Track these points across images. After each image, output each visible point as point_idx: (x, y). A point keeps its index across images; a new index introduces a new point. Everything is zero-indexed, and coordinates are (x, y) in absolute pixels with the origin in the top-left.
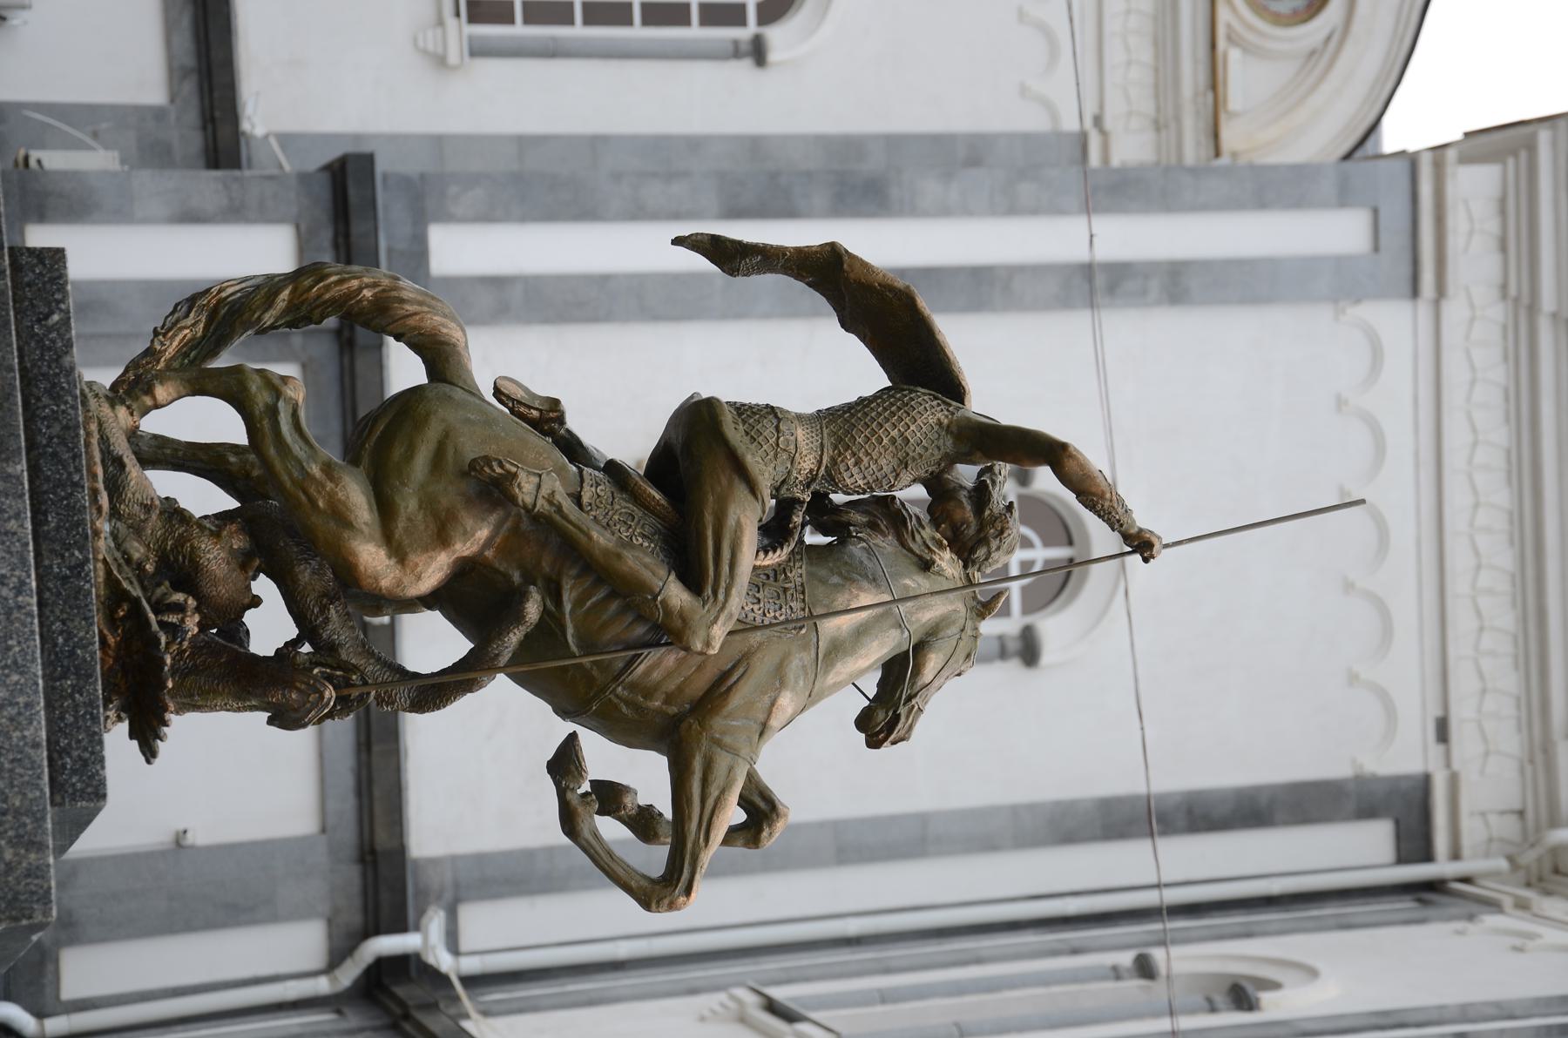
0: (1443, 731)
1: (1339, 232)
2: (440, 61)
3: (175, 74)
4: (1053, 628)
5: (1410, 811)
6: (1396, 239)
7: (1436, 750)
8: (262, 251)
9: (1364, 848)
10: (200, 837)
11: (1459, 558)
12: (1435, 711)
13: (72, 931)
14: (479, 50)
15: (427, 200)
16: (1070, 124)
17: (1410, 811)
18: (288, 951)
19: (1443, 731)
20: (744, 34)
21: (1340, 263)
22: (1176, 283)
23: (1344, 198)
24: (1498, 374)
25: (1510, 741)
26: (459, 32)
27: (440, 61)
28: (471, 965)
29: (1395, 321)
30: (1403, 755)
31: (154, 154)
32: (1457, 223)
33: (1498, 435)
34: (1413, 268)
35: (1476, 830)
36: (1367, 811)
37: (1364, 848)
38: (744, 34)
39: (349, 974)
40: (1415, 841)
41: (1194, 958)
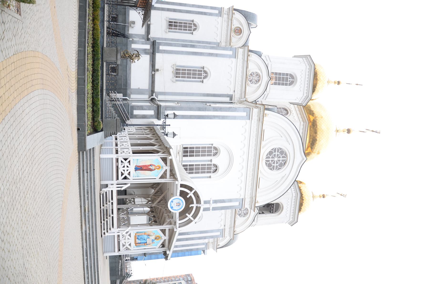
0: (234, 91)
1: (230, 53)
3: (145, 32)
4: (204, 80)
5: (231, 97)
6: (234, 54)
8: (148, 47)
10: (140, 88)
11: (237, 78)
13: (131, 93)
14: (169, 32)
15: (160, 44)
16: (218, 42)
17: (231, 97)
18: (146, 97)
19: (234, 91)
20: (191, 32)
21: (230, 55)
22: (217, 55)
23: (230, 50)
24: (242, 65)
25: (239, 93)
26: (168, 30)
28: (158, 99)
29: (234, 60)
30: (231, 93)
31: (143, 38)
32: (239, 53)
33: (241, 69)
34: (235, 56)
35: (235, 99)
36: (228, 97)
37: (227, 99)
38: (191, 32)
39: (150, 99)
40: (231, 99)
41: (208, 104)
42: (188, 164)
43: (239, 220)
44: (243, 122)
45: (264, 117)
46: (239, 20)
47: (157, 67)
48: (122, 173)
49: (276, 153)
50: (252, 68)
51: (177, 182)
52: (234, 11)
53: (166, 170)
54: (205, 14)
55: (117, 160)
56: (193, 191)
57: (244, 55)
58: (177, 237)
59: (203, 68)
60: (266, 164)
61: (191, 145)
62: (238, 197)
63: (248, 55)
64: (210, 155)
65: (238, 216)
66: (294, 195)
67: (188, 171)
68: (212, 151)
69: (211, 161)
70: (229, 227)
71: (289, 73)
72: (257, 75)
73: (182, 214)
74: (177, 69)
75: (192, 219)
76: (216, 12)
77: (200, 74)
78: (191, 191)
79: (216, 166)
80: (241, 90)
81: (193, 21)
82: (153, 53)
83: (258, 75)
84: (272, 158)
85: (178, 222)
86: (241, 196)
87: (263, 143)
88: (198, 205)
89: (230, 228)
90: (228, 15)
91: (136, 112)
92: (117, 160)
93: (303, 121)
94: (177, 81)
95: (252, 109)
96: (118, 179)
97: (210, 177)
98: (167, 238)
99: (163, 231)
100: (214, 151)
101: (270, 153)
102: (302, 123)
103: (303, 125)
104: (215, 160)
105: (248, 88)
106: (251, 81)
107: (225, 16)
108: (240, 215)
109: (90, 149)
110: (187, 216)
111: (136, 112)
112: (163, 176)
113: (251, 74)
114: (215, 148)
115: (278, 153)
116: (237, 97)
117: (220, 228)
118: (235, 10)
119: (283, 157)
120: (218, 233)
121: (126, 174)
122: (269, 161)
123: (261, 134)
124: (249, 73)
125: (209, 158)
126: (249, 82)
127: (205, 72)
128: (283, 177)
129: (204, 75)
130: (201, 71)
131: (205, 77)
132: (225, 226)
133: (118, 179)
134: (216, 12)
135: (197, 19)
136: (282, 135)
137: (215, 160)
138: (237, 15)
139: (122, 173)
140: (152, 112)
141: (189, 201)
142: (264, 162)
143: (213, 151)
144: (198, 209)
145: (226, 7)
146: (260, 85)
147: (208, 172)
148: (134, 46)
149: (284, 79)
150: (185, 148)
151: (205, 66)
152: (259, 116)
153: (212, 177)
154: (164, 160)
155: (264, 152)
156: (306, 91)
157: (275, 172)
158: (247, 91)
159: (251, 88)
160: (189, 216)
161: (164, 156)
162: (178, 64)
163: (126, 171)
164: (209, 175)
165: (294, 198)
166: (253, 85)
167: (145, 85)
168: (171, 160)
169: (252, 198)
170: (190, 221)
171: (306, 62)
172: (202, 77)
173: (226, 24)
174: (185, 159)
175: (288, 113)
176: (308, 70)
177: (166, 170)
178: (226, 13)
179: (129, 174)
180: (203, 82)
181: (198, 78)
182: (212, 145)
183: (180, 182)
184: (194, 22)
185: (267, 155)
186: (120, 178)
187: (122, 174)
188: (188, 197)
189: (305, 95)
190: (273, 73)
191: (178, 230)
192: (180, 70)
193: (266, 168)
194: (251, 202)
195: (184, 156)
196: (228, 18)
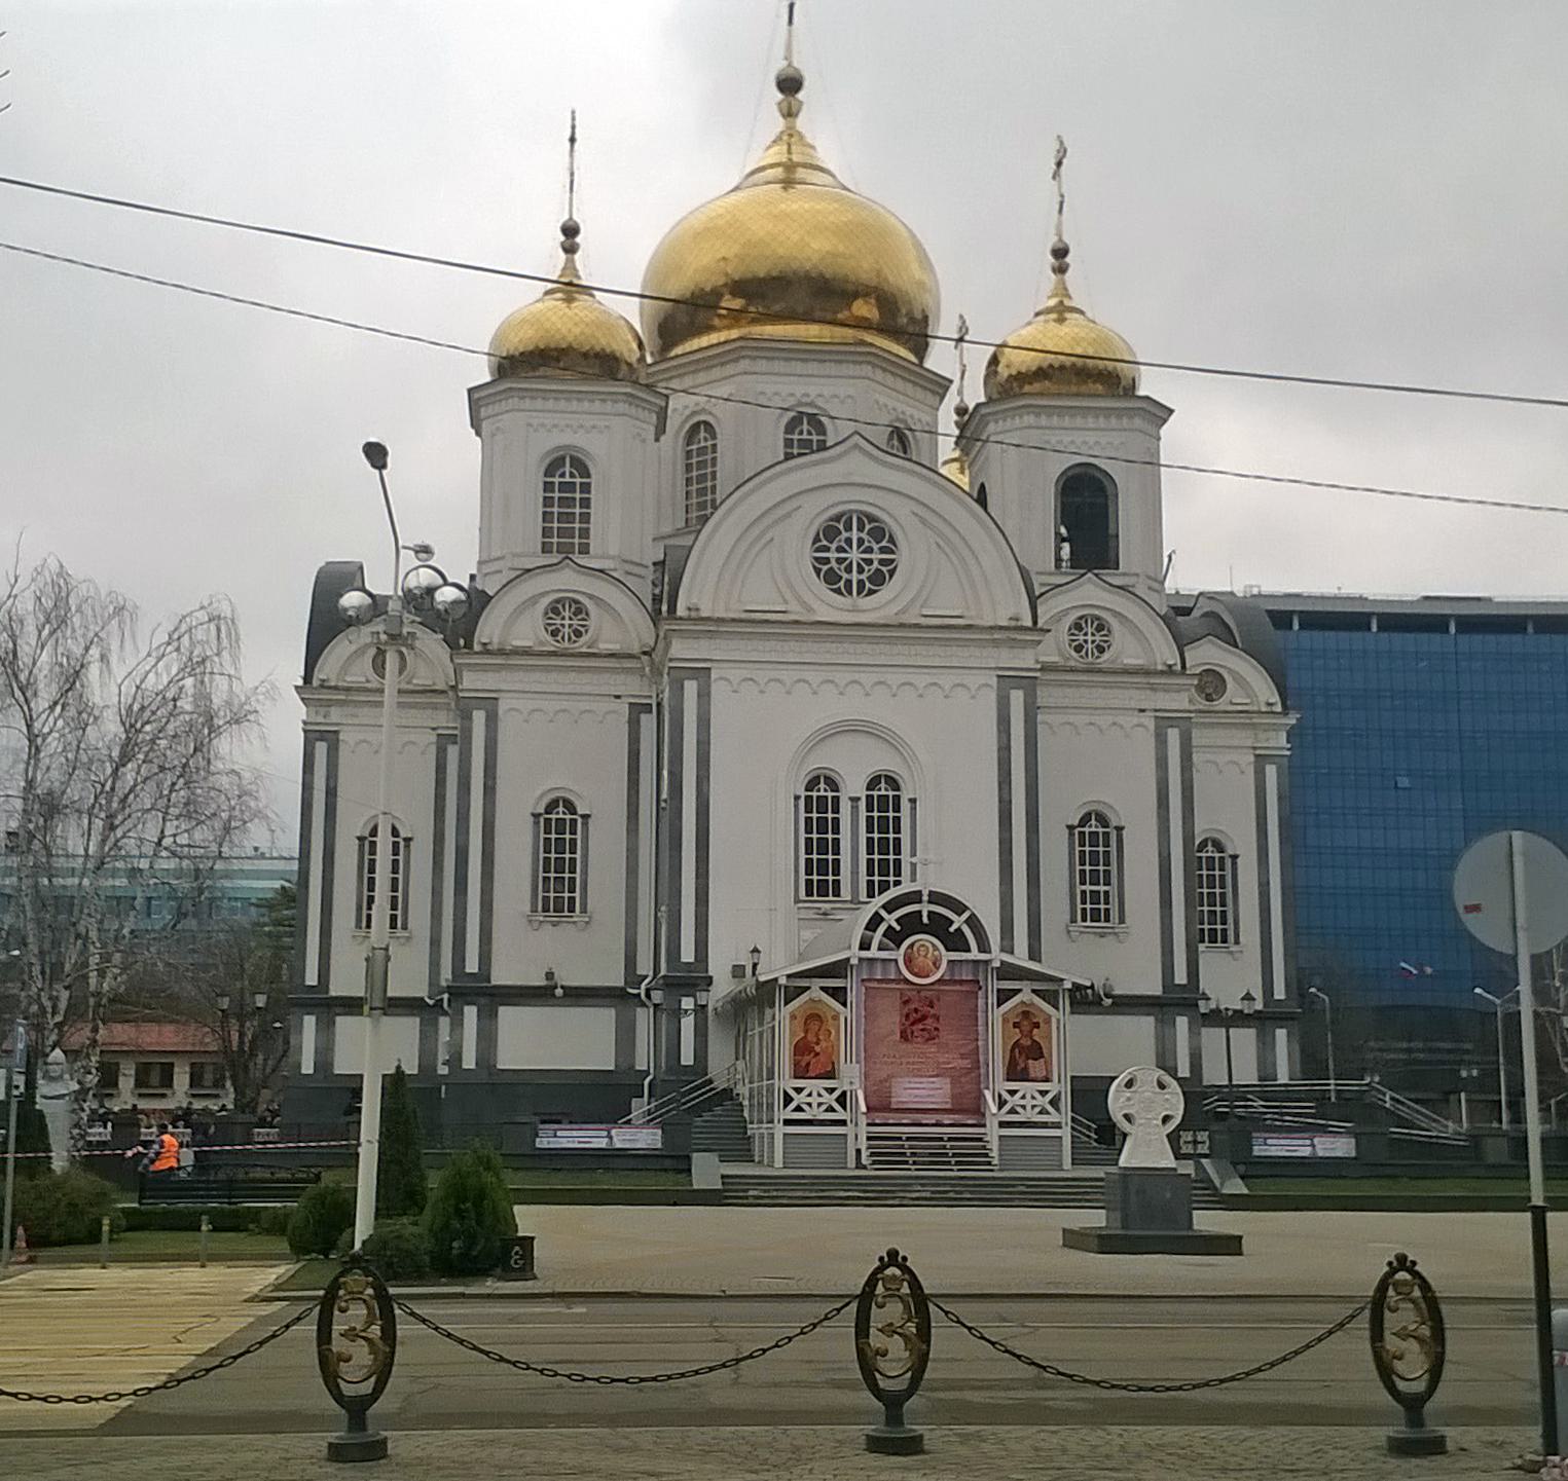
0: (618, 697)
2: (408, 939)
5: (637, 710)
7: (623, 699)
8: (470, 1013)
9: (648, 722)
12: (613, 699)
16: (433, 739)
19: (618, 697)
20: (402, 844)
27: (408, 939)
28: (651, 973)
37: (648, 722)
38: (402, 844)
40: (647, 708)
42: (863, 878)
43: (1125, 650)
44: (718, 690)
45: (704, 614)
46: (345, 657)
47: (539, 981)
48: (826, 1110)
49: (833, 555)
50: (529, 632)
51: (854, 961)
52: (315, 683)
53: (822, 988)
54: (331, 793)
55: (787, 1122)
56: (883, 913)
57: (485, 668)
58: (1020, 958)
59: (536, 816)
60: (871, 592)
61: (797, 871)
62: (992, 697)
63: (486, 651)
64: (836, 800)
65: (1106, 656)
66: (1029, 419)
67: (892, 879)
69: (855, 800)
70: (1148, 692)
71: (541, 479)
73: (956, 942)
74: (546, 909)
75: (966, 915)
76: (321, 749)
77: (560, 826)
78: (882, 919)
79: (873, 783)
80: (613, 670)
81: (361, 839)
82: (494, 998)
83: (554, 609)
84: (849, 570)
85: (975, 954)
86: (987, 685)
87: (796, 612)
88: (925, 898)
89: (1152, 689)
90: (330, 703)
91: (687, 1058)
92: (787, 1122)
93: (736, 360)
94: (584, 910)
95: (671, 660)
96: (843, 1123)
97: (913, 801)
98: (1026, 987)
99: (1004, 996)
100: (823, 790)
101: (831, 578)
102: (744, 364)
103: (754, 358)
105: (603, 647)
106: (578, 634)
107: (336, 715)
108: (1101, 650)
109: (723, 1183)
110: (959, 930)
111: (687, 1058)
112: (839, 994)
113: (554, 634)
114: (811, 785)
115: (833, 546)
116: (634, 687)
117: (1152, 727)
118: (308, 678)
120: (1173, 736)
121: (831, 1099)
122: (861, 583)
124: (551, 644)
126: (583, 640)
127: (551, 807)
128: (923, 521)
129: (561, 813)
130: (548, 821)
131: (570, 807)
132: (1143, 711)
133: (843, 1123)
134: (321, 749)
135: (349, 829)
136: (768, 537)
137: (854, 786)
138: (327, 669)
139: (826, 1110)
141: (911, 925)
142: (866, 602)
143: (822, 793)
144: (935, 898)
145: (301, 711)
146: (591, 597)
147: (897, 809)
148: (469, 1062)
149: (566, 486)
150: (809, 893)
151: (531, 810)
152: (696, 635)
153: (912, 796)
154: (792, 994)
155: (828, 606)
156: (609, 407)
157: (903, 557)
158: (614, 647)
159: (605, 634)
160: (958, 922)
161: (780, 997)
162: (527, 908)
163: (821, 1100)
164: (905, 805)
165: (1043, 421)
166: (592, 623)
167: (601, 1021)
168: (789, 976)
169: (996, 643)
170: (973, 922)
171: (497, 408)
173: (366, 710)
174: (846, 894)
175: (706, 423)
176: (527, 404)
177: (822, 988)
178: (322, 710)
179: (831, 1091)
180: (585, 817)
181: (573, 832)
182: (797, 798)
183: (854, 954)
185: (838, 591)
186: (840, 1115)
187: (831, 1109)
188: (898, 928)
189: (622, 407)
190: (546, 549)
191: (997, 956)
192: (546, 900)
193: (886, 592)
194: (1013, 644)
195: (837, 893)
196: (342, 703)
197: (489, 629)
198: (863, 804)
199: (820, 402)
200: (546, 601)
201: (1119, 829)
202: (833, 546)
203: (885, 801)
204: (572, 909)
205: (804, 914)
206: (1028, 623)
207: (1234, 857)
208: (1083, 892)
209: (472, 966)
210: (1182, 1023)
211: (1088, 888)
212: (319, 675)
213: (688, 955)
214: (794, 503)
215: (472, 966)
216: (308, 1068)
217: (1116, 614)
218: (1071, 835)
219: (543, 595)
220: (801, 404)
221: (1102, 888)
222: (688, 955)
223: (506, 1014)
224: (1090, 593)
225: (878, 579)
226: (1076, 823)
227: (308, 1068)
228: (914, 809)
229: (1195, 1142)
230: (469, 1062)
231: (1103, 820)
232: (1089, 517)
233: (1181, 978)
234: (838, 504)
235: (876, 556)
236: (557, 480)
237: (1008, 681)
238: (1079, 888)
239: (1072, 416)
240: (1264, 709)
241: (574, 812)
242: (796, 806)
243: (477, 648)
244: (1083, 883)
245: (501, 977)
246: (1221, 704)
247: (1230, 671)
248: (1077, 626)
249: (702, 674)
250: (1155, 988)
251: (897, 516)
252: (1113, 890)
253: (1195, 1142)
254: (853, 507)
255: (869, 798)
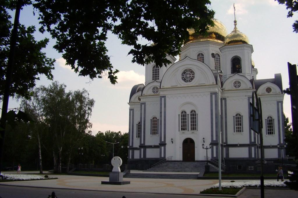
8: (142, 150)
43: (243, 86)
44: (167, 99)
50: (150, 92)
52: (130, 102)
65: (240, 87)
66: (226, 50)
68: (184, 115)
69: (188, 115)
71: (152, 69)
72: (154, 89)
79: (192, 112)
81: (137, 124)
83: (154, 89)
87: (179, 86)
91: (163, 156)
97: (197, 114)
101: (184, 80)
104: (188, 112)
106: (157, 92)
108: (239, 86)
111: (163, 156)
114: (182, 112)
119: (187, 72)
123: (174, 88)
125: (187, 115)
127: (154, 118)
129: (155, 119)
130: (153, 121)
134: (132, 111)
137: (188, 112)
140: (163, 148)
151: (150, 119)
157: (195, 75)
172: (156, 120)
182: (179, 115)
184: (138, 123)
190: (153, 79)
193: (193, 81)
197: (145, 92)
198: (190, 116)
199: (202, 51)
200: (152, 87)
201: (242, 116)
202: (185, 75)
203: (194, 114)
204: (156, 134)
205: (181, 133)
206: (215, 83)
207: (274, 119)
208: (236, 127)
209: (142, 143)
210: (253, 148)
211: (237, 126)
212: (131, 101)
213: (163, 140)
214: (178, 69)
215: (142, 143)
216: (131, 158)
217: (241, 80)
218: (234, 118)
219: (152, 86)
220: (199, 52)
221: (240, 126)
222: (163, 140)
223: (148, 150)
224: (237, 77)
225: (192, 79)
226: (235, 115)
227: (131, 158)
228: (197, 115)
229: (251, 168)
230: (142, 157)
231: (240, 115)
232: (236, 65)
233: (253, 140)
234: (185, 68)
235: (191, 76)
236: (154, 69)
237: (212, 94)
238: (235, 126)
239: (231, 48)
240: (279, 93)
241: (157, 119)
242: (179, 116)
243: (143, 95)
244: (236, 125)
245: (146, 144)
246: (271, 93)
247: (272, 87)
248: (235, 83)
249: (164, 97)
250: (248, 142)
251: (194, 69)
252: (241, 126)
253: (251, 168)
254: (187, 68)
255: (191, 114)
